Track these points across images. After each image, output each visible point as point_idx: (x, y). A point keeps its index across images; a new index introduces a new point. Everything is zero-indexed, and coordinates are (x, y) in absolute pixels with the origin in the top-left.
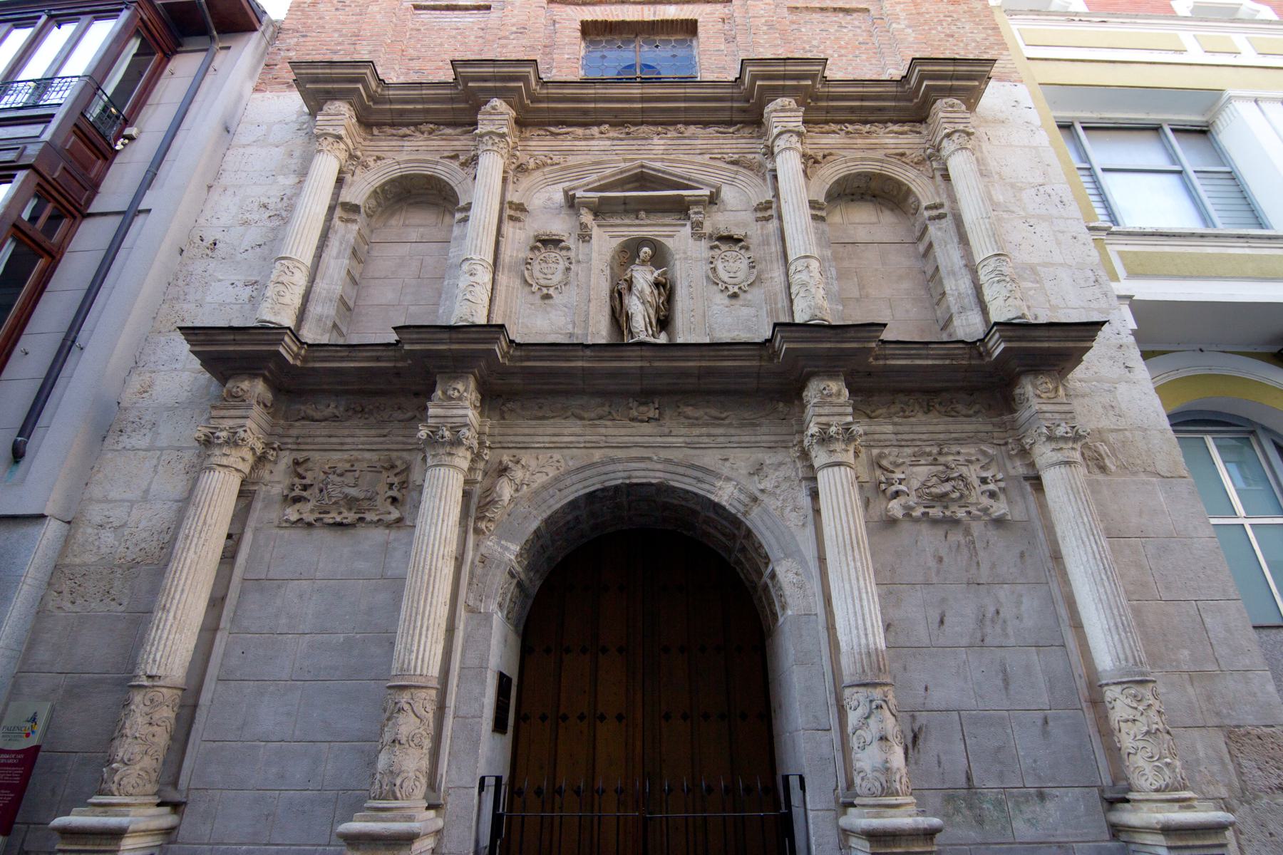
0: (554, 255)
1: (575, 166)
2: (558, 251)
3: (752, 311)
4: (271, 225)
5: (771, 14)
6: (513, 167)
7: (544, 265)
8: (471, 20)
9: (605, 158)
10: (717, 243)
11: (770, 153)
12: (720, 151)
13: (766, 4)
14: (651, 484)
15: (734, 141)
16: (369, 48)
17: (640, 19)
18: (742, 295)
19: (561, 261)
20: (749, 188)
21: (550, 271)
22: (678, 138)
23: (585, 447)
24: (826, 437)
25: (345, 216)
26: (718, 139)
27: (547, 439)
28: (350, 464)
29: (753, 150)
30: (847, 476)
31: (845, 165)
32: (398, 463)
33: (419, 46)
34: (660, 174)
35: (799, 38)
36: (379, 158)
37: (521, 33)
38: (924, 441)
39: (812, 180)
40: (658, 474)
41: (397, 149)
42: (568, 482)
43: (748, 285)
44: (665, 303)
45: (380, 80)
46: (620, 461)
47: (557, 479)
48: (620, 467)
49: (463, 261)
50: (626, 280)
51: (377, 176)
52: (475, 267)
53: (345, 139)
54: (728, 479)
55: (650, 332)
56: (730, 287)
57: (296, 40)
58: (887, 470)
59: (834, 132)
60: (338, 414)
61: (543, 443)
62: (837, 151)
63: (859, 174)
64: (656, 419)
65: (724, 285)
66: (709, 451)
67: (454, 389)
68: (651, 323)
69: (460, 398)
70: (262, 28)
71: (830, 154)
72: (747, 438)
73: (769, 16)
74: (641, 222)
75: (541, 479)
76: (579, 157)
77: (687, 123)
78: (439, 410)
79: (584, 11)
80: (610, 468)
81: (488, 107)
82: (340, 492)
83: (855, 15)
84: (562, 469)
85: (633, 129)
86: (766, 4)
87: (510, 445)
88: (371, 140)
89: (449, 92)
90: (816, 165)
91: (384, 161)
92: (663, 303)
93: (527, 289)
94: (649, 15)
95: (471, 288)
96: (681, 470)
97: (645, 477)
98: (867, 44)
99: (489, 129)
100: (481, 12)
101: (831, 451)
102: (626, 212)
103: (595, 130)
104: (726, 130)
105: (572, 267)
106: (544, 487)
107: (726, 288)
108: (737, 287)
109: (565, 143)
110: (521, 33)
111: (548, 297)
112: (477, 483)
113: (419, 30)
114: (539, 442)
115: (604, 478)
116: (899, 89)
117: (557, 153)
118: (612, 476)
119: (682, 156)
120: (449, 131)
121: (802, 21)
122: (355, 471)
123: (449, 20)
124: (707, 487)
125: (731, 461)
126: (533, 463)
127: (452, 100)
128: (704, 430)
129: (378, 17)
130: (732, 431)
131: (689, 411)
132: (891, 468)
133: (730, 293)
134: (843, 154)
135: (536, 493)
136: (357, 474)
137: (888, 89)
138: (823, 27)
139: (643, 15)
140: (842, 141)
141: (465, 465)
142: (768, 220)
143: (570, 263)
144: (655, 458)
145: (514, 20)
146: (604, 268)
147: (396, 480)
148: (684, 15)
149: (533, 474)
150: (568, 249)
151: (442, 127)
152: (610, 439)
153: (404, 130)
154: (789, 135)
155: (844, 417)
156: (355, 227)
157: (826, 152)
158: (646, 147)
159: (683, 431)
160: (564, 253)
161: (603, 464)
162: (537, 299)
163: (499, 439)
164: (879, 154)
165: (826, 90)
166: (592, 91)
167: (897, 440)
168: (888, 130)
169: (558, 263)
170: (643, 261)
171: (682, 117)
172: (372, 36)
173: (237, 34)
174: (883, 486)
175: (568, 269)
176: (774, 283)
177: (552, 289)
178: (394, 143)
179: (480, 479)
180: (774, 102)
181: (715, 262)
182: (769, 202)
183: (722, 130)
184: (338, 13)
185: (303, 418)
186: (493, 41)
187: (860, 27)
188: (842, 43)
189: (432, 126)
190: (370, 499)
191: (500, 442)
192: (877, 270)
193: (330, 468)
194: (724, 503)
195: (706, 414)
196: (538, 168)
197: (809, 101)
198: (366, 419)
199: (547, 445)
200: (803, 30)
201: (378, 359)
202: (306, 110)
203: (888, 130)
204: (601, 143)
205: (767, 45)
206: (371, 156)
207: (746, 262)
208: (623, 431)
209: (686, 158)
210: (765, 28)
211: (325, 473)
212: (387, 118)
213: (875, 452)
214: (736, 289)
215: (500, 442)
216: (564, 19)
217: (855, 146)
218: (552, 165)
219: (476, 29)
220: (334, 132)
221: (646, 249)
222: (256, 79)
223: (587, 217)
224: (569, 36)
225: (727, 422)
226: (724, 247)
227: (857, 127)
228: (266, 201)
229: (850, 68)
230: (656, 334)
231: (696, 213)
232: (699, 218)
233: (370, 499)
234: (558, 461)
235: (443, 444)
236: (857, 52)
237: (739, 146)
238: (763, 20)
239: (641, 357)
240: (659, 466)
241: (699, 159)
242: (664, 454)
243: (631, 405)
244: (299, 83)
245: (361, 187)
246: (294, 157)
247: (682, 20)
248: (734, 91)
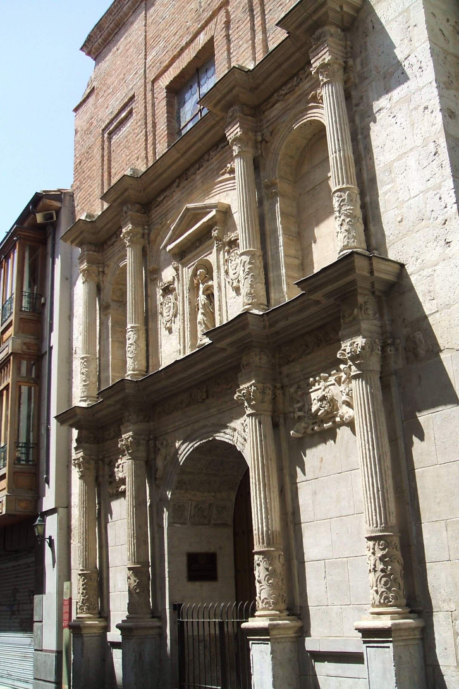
38: (316, 371)
88: (105, 254)
178: (111, 251)
217: (289, 107)
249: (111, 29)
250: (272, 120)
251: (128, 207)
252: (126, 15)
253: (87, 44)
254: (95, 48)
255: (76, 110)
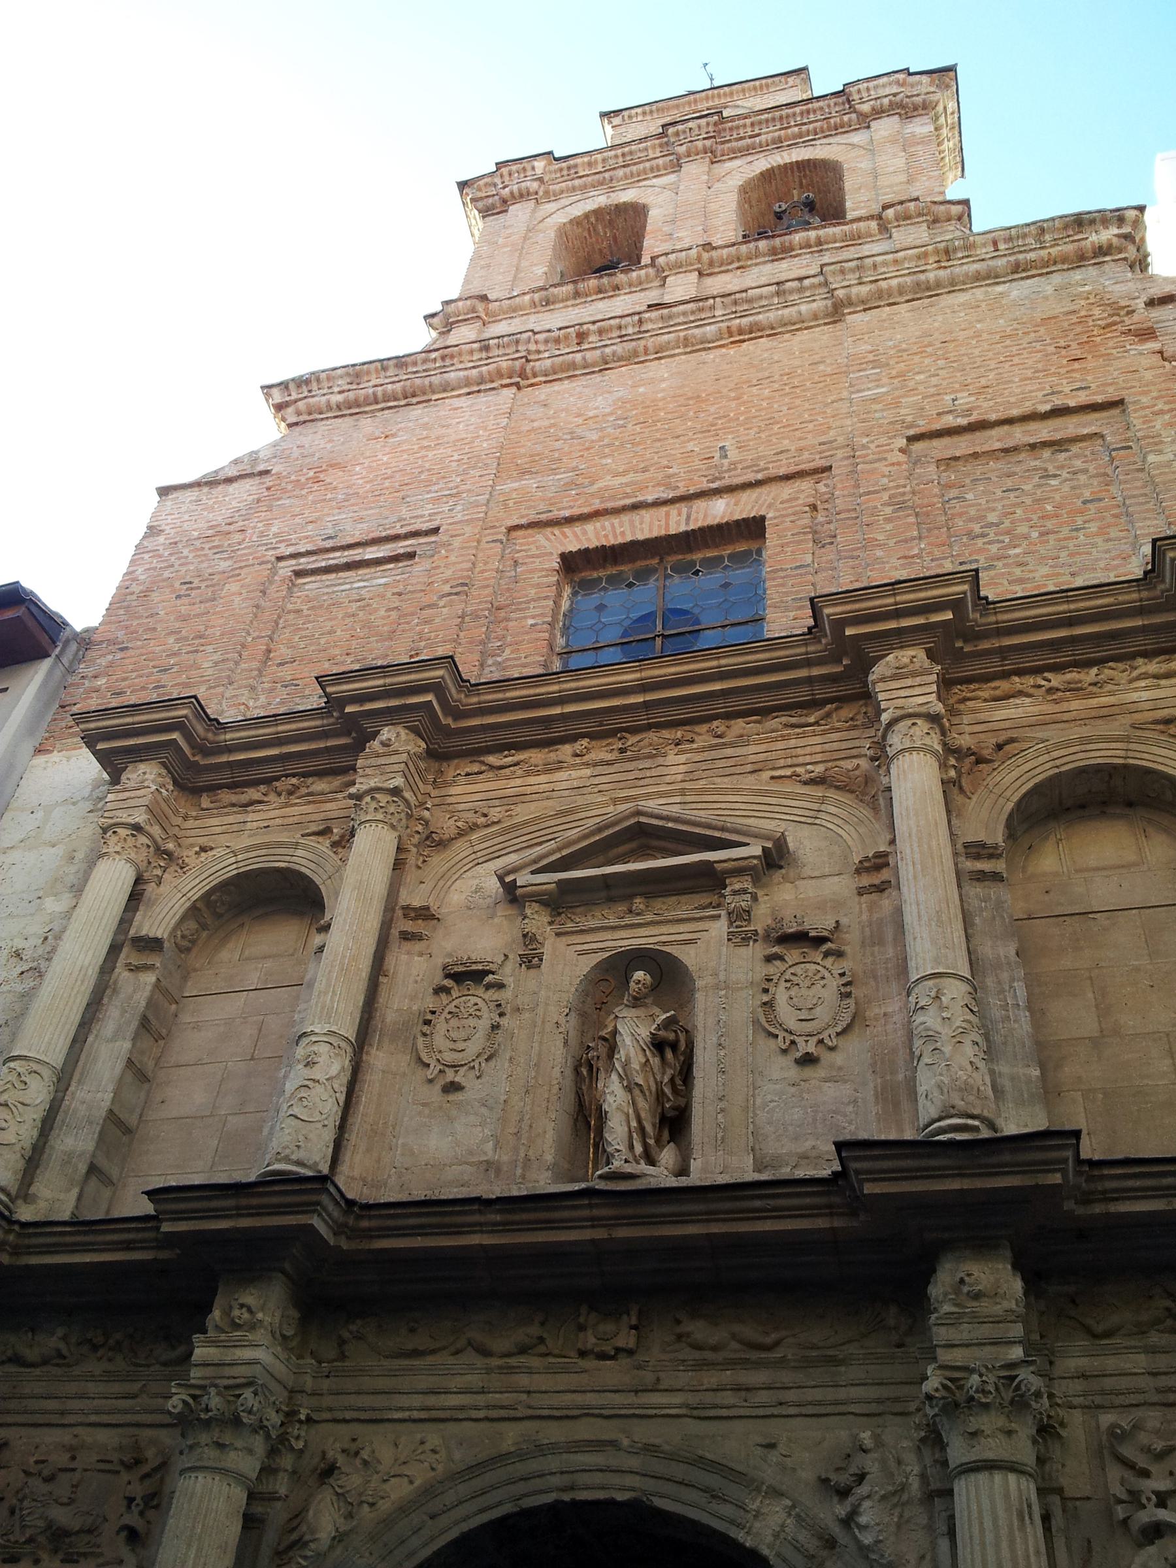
0: (473, 1000)
1: (525, 823)
2: (480, 991)
3: (845, 1090)
4: (19, 988)
5: (902, 482)
6: (416, 839)
7: (454, 1022)
8: (382, 581)
9: (580, 801)
10: (776, 949)
11: (881, 757)
12: (789, 761)
13: (893, 464)
14: (612, 1502)
15: (818, 740)
16: (216, 657)
17: (663, 533)
18: (826, 1057)
19: (485, 1013)
20: (846, 827)
21: (463, 1034)
22: (713, 747)
23: (487, 1419)
24: (960, 1397)
25: (135, 960)
26: (784, 738)
27: (417, 1400)
28: (68, 1456)
29: (855, 752)
30: (1007, 1496)
31: (1046, 757)
32: (150, 1453)
33: (296, 639)
34: (670, 825)
35: (961, 515)
36: (204, 849)
37: (456, 594)
39: (975, 798)
40: (629, 1480)
41: (235, 828)
42: (449, 1498)
43: (838, 1034)
44: (678, 1082)
45: (210, 720)
46: (553, 1448)
47: (429, 1492)
48: (553, 1463)
49: (300, 1037)
50: (604, 1039)
51: (197, 881)
52: (315, 1048)
53: (147, 828)
54: (776, 1493)
55: (639, 1148)
56: (800, 1041)
57: (110, 657)
58: (1129, 1465)
59: (1021, 693)
60: (65, 1352)
61: (409, 1409)
62: (1029, 733)
63: (1082, 771)
64: (630, 1352)
65: (789, 1037)
66: (738, 1426)
67: (242, 1306)
68: (642, 1129)
69: (253, 1326)
70: (58, 650)
71: (1012, 740)
72: (818, 1394)
73: (898, 487)
74: (637, 920)
75: (399, 1491)
76: (533, 806)
77: (729, 716)
78: (212, 1350)
79: (565, 536)
80: (533, 1466)
81: (375, 744)
82: (40, 1518)
83: (1075, 449)
84: (440, 1468)
85: (632, 739)
86: (893, 464)
87: (348, 1415)
88: (196, 818)
89: (318, 723)
90: (981, 766)
91: (210, 853)
92: (672, 1080)
93: (421, 1073)
94: (678, 523)
95: (303, 1093)
96: (679, 1471)
97: (603, 1488)
98: (1100, 500)
99: (373, 783)
100: (401, 565)
101: (974, 1434)
102: (611, 900)
103: (567, 749)
104: (803, 720)
105: (504, 1022)
106: (404, 1509)
107: (793, 1042)
108: (815, 1039)
109: (513, 783)
110: (456, 594)
111: (453, 1087)
112: (279, 1499)
113: (298, 611)
114: (402, 1409)
115: (521, 1488)
116: (1145, 594)
117: (497, 802)
118: (537, 1484)
119: (718, 780)
120: (320, 785)
121: (968, 481)
122: (73, 1470)
123: (348, 586)
124: (727, 1510)
125: (782, 1448)
126: (386, 1455)
127: (324, 735)
128: (727, 1376)
129: (237, 599)
130: (786, 1377)
131: (698, 1329)
132: (1142, 1462)
133: (798, 1055)
134: (1039, 735)
135: (388, 1522)
136: (77, 1476)
137: (1120, 598)
138: (1009, 483)
139: (667, 524)
140: (1036, 710)
141: (249, 1466)
142: (882, 891)
143: (501, 1015)
144: (626, 1442)
145: (449, 573)
146: (562, 1020)
147: (138, 1490)
148: (741, 512)
149: (385, 1481)
150: (500, 986)
151: (310, 780)
152: (536, 1400)
153: (253, 794)
154: (909, 722)
155: (1002, 1349)
156: (150, 978)
157: (1002, 737)
158: (654, 773)
159: (684, 1378)
160: (492, 994)
161: (521, 1456)
162: (434, 1094)
163: (328, 1401)
164: (1117, 727)
165: (992, 619)
166: (555, 688)
167: (1159, 1391)
168: (1135, 673)
169: (479, 1017)
170: (635, 998)
171: (720, 707)
172: (222, 635)
173: (24, 665)
174: (1120, 1512)
175: (495, 1027)
176: (890, 1027)
177: (462, 1070)
179: (283, 1491)
180: (883, 662)
181: (772, 990)
182: (885, 855)
183: (793, 720)
184: (179, 602)
185: (10, 1360)
186: (412, 614)
187: (1085, 471)
188: (1049, 508)
189: (294, 781)
190: (90, 1531)
191: (330, 1409)
192: (1137, 969)
193: (37, 1462)
194: (766, 1551)
195: (734, 1336)
196: (462, 833)
197: (959, 644)
198: (110, 1360)
199: (416, 1415)
200: (970, 496)
201: (128, 1246)
202: (106, 776)
203: (1135, 673)
204: (574, 774)
205: (891, 543)
206: (192, 845)
207: (834, 983)
208: (563, 1381)
209: (725, 782)
210: (889, 510)
211: (27, 1473)
212: (225, 777)
213: (1107, 1419)
214: (811, 1048)
215: (330, 1409)
216: (532, 556)
217: (1066, 717)
218: (487, 826)
219: (389, 595)
220: (130, 820)
221: (639, 975)
222: (41, 733)
223: (538, 920)
224: (538, 585)
225: (777, 1354)
226: (793, 955)
227: (1069, 676)
228: (19, 943)
229: (1064, 554)
230: (654, 1151)
231: (735, 893)
232: (743, 902)
233: (90, 1531)
234: (434, 1451)
235: (207, 1424)
236: (1079, 521)
237: (827, 747)
238: (885, 496)
239: (592, 1219)
240: (634, 1462)
241: (749, 782)
242: (644, 1432)
243: (582, 1320)
244: (90, 741)
245: (170, 905)
246: (76, 861)
247: (737, 522)
248: (811, 648)
249: (385, 393)
250: (996, 726)
251: (398, 735)
252: (446, 388)
253: (292, 386)
254: (308, 405)
255: (164, 492)
